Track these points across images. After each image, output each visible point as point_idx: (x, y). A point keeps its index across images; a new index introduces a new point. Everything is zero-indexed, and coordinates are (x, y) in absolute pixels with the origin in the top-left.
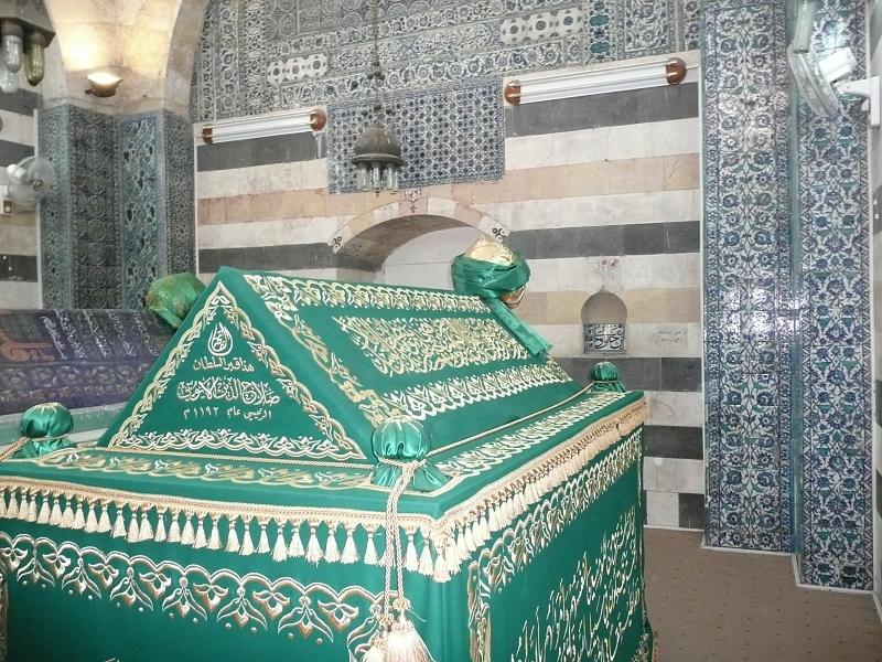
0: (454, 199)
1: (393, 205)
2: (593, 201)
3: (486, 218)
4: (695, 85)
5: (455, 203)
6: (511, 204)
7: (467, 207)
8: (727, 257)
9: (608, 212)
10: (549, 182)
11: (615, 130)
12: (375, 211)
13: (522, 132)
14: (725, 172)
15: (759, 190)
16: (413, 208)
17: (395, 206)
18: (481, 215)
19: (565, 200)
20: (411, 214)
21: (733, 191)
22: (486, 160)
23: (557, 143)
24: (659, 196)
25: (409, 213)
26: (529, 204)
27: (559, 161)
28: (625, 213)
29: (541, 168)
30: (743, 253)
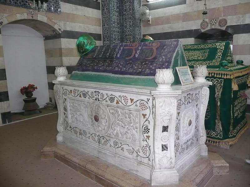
0: (46, 17)
1: (24, 14)
2: (82, 25)
3: (57, 25)
4: (100, 2)
5: (47, 18)
6: (63, 22)
7: (51, 20)
8: (114, 43)
9: (85, 29)
10: (71, 18)
11: (86, 8)
12: (17, 15)
13: (65, 2)
14: (113, 25)
15: (118, 30)
16: (32, 17)
17: (25, 14)
18: (55, 23)
19: (76, 24)
20: (32, 18)
21: (114, 29)
22: (55, 7)
23: (74, 7)
24: (94, 27)
25: (31, 18)
26: (68, 23)
27: (74, 12)
28: (89, 30)
29: (71, 14)
30: (116, 42)
